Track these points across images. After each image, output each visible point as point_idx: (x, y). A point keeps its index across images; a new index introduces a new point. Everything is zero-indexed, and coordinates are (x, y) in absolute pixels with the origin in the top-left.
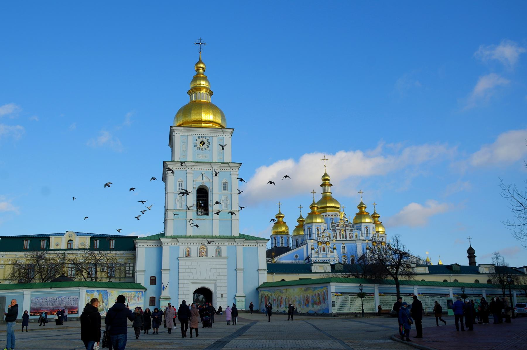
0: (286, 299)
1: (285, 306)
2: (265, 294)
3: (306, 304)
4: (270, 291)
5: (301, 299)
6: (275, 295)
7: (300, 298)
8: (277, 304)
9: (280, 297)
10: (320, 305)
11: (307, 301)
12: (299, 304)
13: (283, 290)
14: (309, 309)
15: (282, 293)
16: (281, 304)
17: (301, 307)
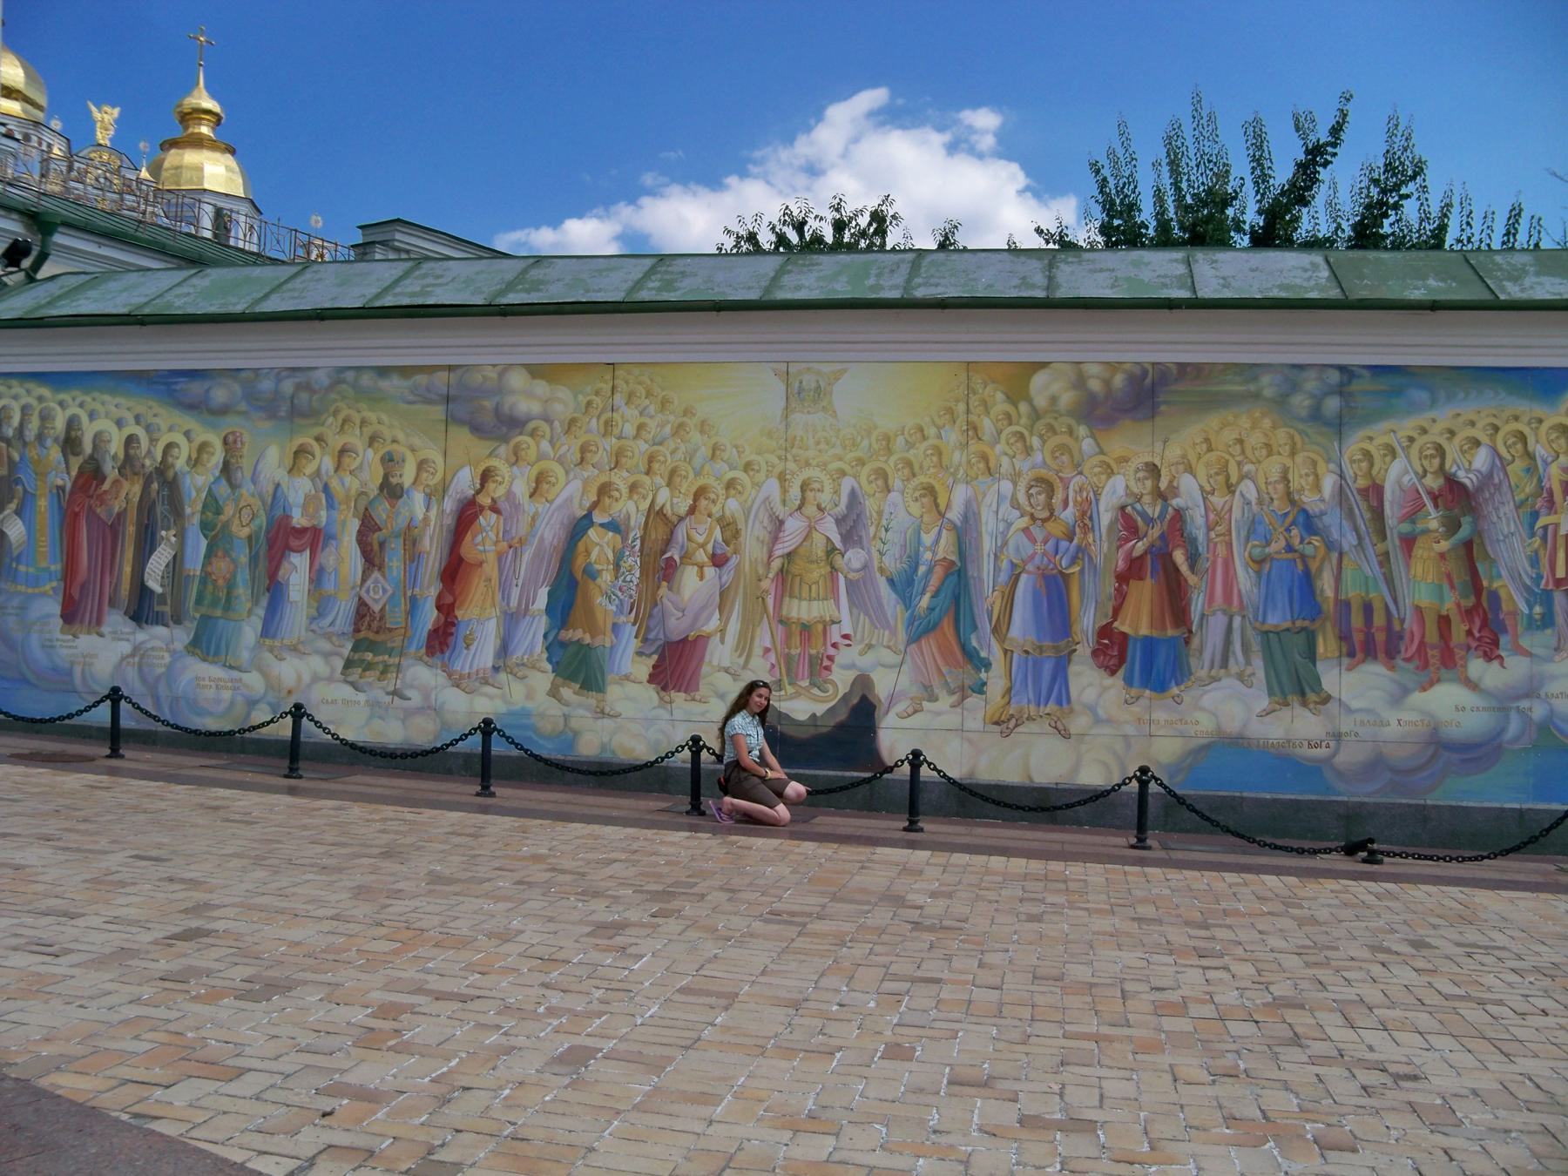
0: (578, 528)
1: (555, 647)
2: (70, 443)
3: (1105, 631)
4: (195, 388)
5: (987, 545)
6: (328, 463)
7: (965, 534)
8: (343, 610)
9: (435, 494)
10: (1476, 666)
11: (1144, 593)
12: (920, 630)
13: (517, 380)
14: (1203, 724)
15: (477, 429)
16: (446, 609)
17: (980, 688)
